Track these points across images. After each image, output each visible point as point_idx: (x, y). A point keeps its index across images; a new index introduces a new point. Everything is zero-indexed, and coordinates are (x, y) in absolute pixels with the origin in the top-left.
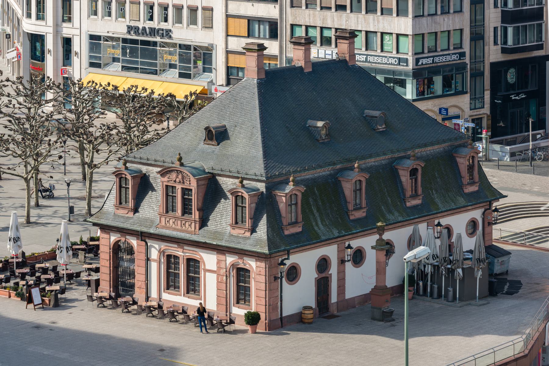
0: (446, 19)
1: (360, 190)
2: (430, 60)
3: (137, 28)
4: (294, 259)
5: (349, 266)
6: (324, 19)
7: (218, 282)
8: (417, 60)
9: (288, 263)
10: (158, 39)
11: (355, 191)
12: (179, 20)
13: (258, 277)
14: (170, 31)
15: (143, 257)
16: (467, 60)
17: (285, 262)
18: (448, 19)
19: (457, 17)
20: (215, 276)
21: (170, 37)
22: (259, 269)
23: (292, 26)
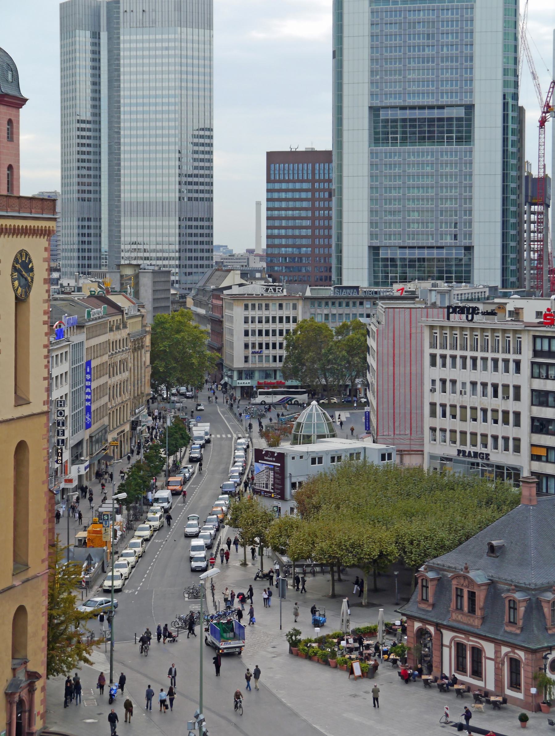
3: (464, 452)
10: (479, 460)
13: (526, 667)
15: (439, 643)
20: (493, 662)
21: (489, 459)
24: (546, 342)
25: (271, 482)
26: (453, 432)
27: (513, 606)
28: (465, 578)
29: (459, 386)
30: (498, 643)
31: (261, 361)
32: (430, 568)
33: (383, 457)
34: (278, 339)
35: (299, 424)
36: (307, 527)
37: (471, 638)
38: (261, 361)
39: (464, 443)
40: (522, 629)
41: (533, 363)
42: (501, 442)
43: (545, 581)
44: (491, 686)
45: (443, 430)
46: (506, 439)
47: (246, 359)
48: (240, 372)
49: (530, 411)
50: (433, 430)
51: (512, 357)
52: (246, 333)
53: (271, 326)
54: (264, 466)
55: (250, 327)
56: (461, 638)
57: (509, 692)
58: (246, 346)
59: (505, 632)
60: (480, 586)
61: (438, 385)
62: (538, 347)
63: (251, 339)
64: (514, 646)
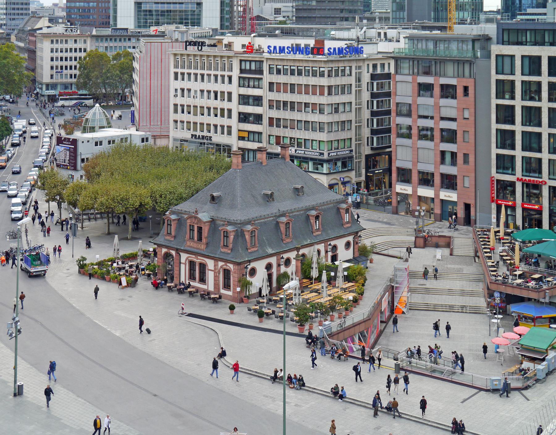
1: (289, 227)
2: (335, 154)
3: (196, 136)
4: (253, 265)
6: (284, 133)
7: (214, 276)
8: (329, 154)
10: (205, 141)
11: (286, 228)
14: (211, 137)
16: (354, 153)
18: (344, 133)
19: (349, 132)
20: (213, 272)
21: (211, 140)
23: (269, 135)
24: (248, 63)
25: (68, 159)
26: (189, 123)
27: (226, 236)
29: (192, 93)
30: (216, 259)
31: (62, 78)
32: (173, 213)
33: (143, 140)
34: (74, 63)
35: (87, 119)
36: (91, 188)
37: (199, 257)
38: (62, 78)
39: (195, 129)
40: (232, 250)
41: (240, 78)
42: (219, 128)
43: (247, 218)
44: (211, 288)
45: (182, 122)
46: (222, 127)
47: (52, 76)
48: (47, 85)
49: (238, 108)
50: (176, 121)
51: (226, 73)
52: (52, 59)
53: (69, 55)
54: (63, 148)
55: (55, 55)
56: (193, 258)
57: (223, 291)
58: (52, 68)
59: (221, 252)
60: (205, 223)
61: (179, 92)
62: (243, 67)
63: (55, 63)
64: (226, 261)
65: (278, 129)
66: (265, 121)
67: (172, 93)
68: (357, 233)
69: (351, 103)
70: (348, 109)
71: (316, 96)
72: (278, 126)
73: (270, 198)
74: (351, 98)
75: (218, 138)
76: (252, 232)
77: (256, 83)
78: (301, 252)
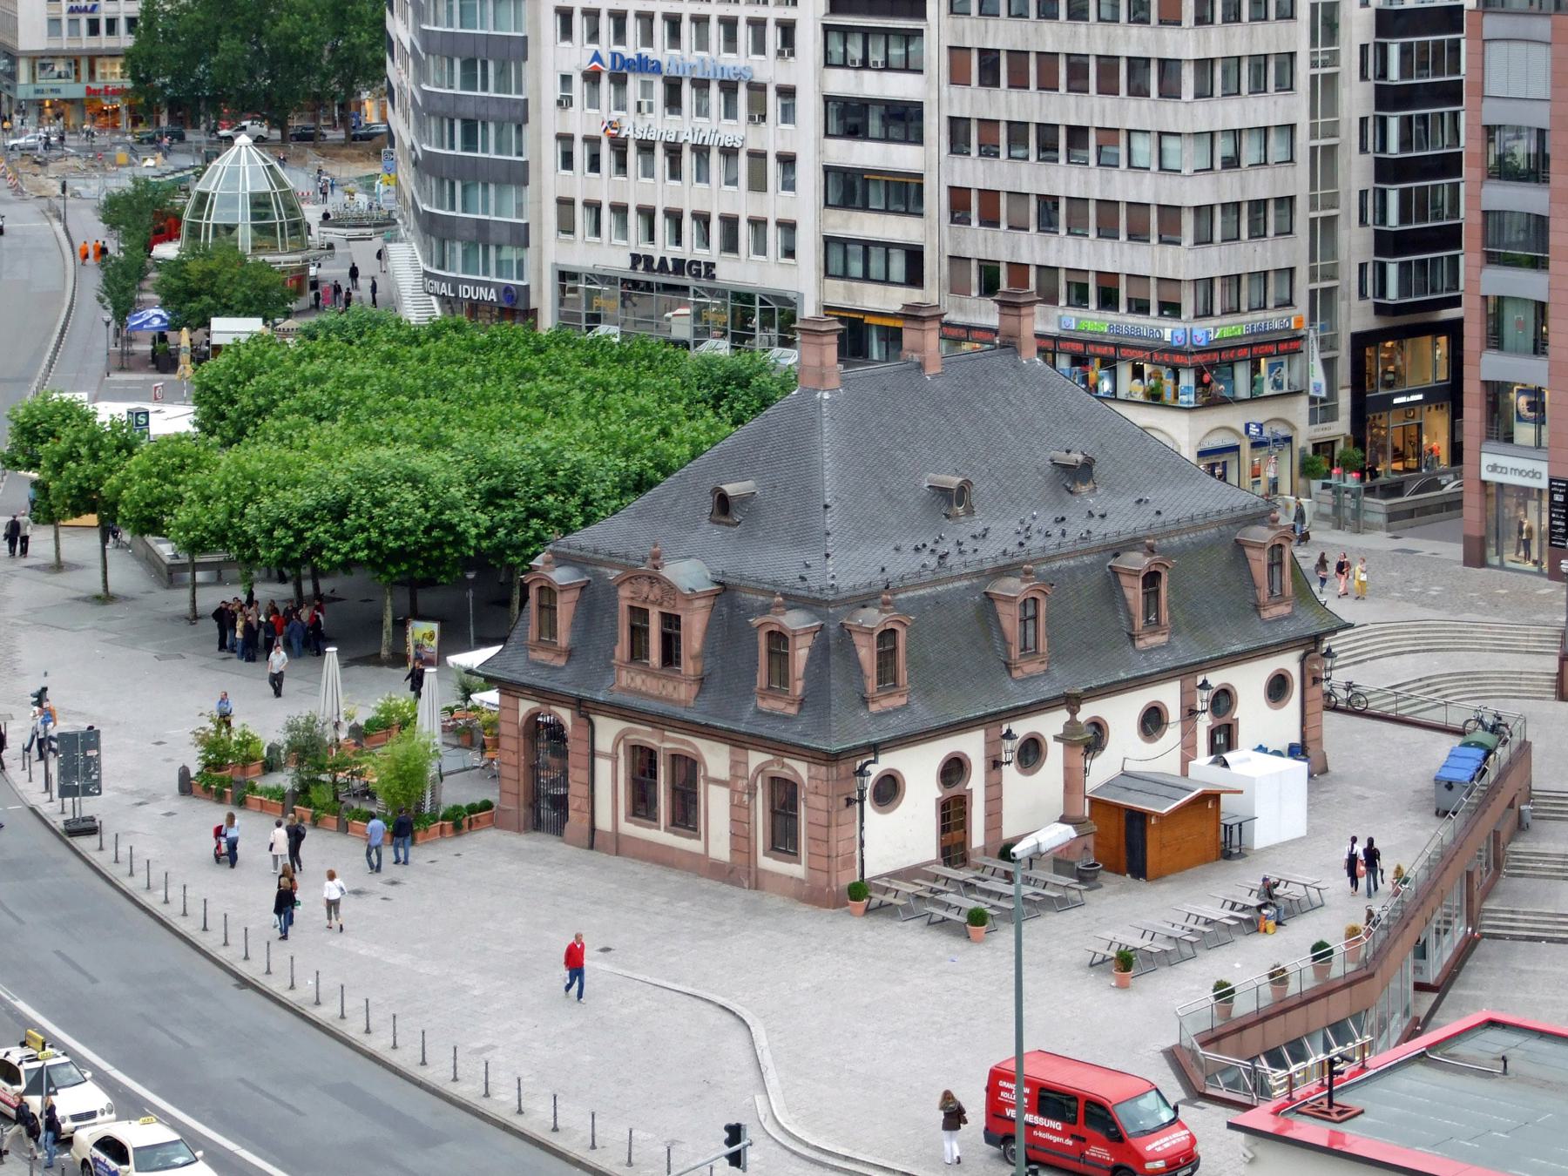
0: (1259, 249)
1: (1035, 618)
3: (649, 260)
4: (887, 762)
5: (1010, 773)
6: (1015, 248)
7: (732, 805)
9: (875, 771)
10: (687, 280)
11: (1024, 621)
12: (731, 244)
13: (812, 797)
14: (714, 265)
15: (584, 748)
17: (868, 768)
21: (713, 277)
22: (814, 783)
28: (654, 579)
30: (737, 740)
32: (561, 560)
35: (203, 198)
40: (802, 703)
50: (565, 204)
56: (646, 735)
59: (759, 712)
60: (694, 595)
65: (989, 231)
66: (936, 200)
67: (551, 90)
68: (1317, 639)
69: (1292, 127)
70: (1277, 149)
71: (1144, 102)
72: (990, 220)
73: (953, 499)
74: (1295, 107)
75: (738, 271)
76: (888, 635)
77: (896, 52)
78: (1086, 712)
